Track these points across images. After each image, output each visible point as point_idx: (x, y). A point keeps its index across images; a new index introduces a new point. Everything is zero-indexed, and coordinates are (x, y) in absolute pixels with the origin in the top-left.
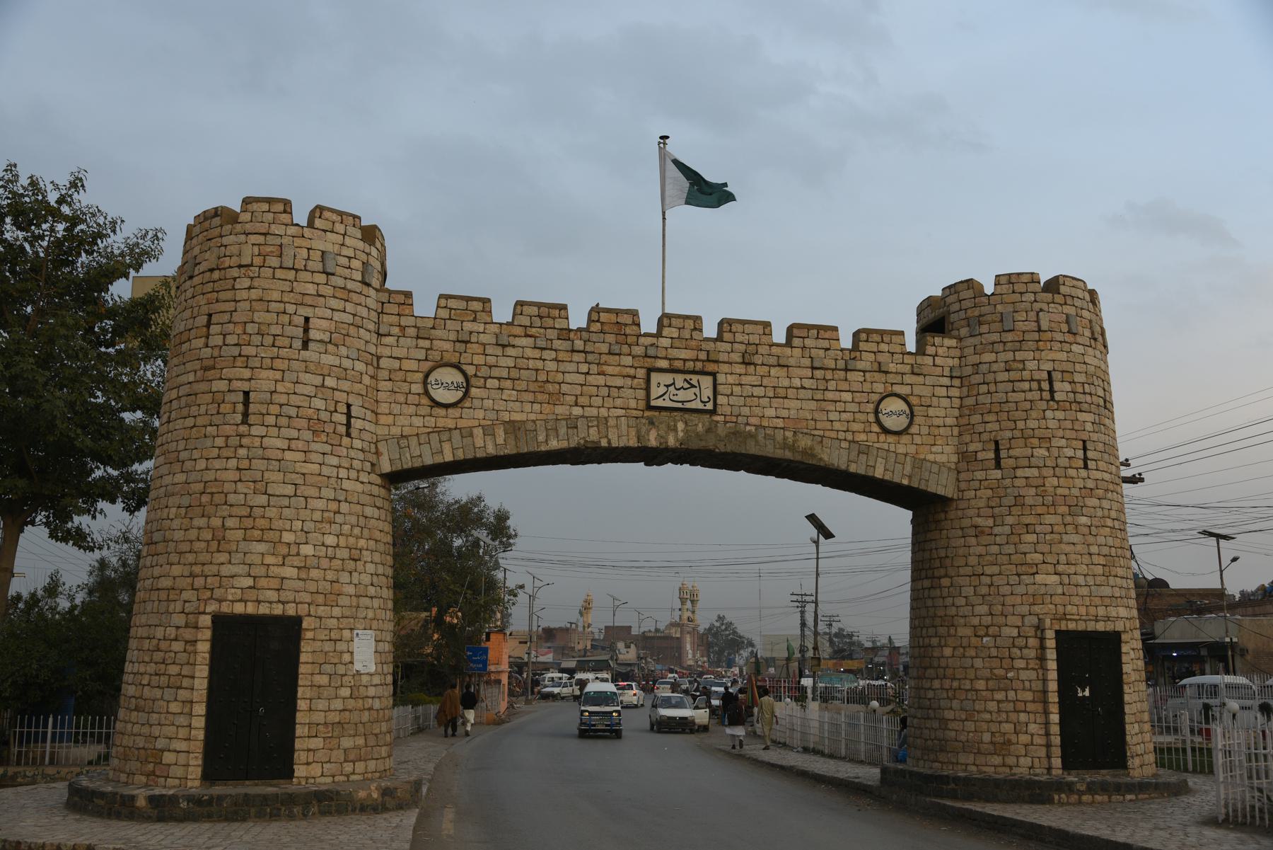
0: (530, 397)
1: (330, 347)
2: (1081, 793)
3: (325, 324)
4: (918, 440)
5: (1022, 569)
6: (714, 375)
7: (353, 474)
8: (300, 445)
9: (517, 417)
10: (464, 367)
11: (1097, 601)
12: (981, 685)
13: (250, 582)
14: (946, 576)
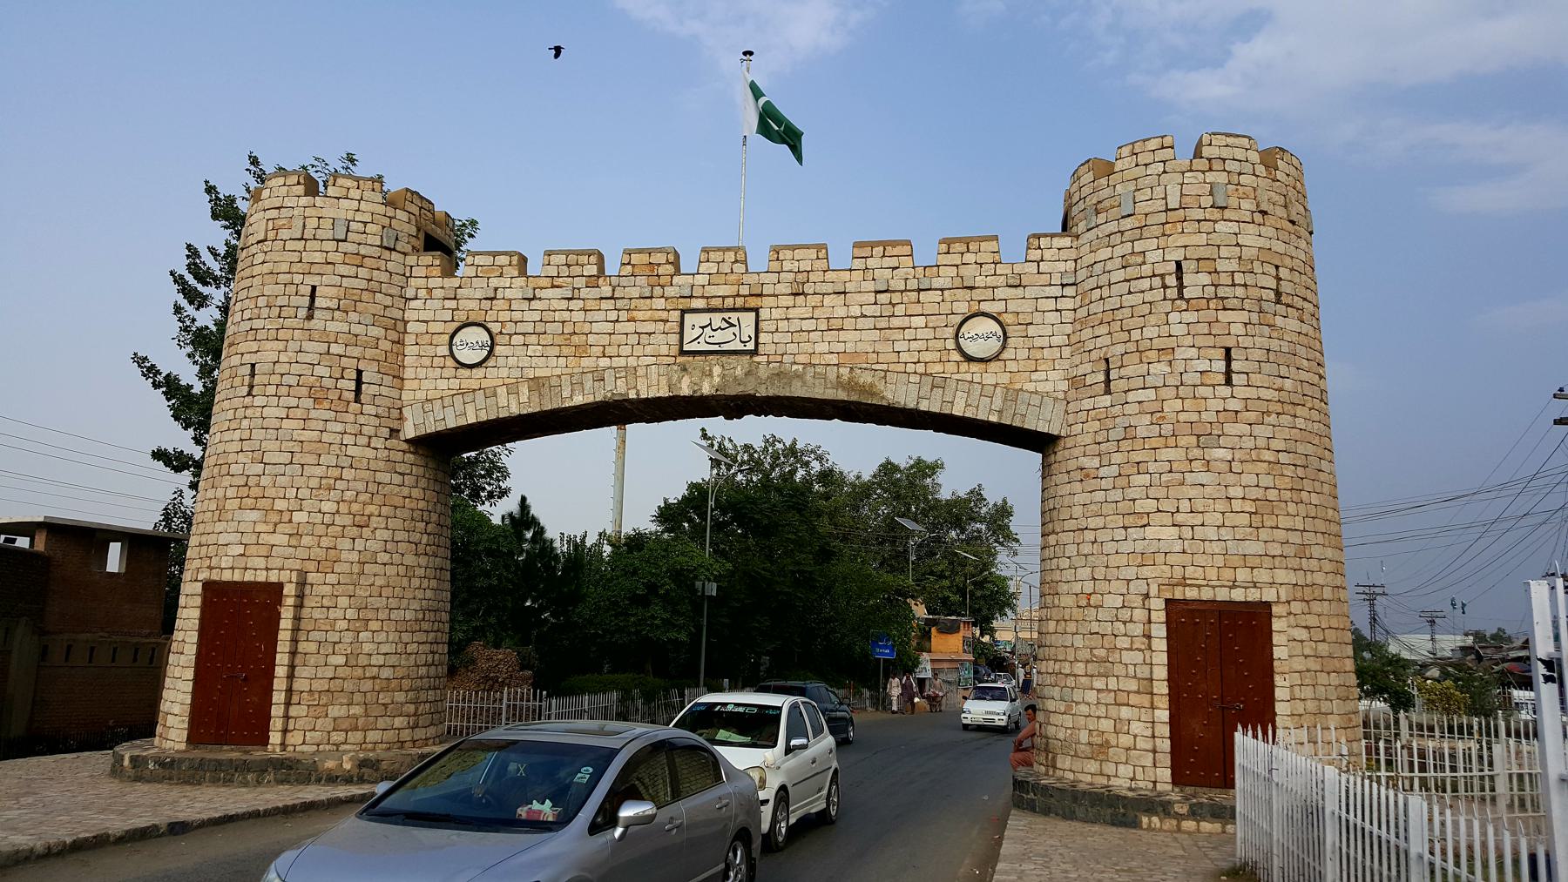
0: (556, 351)
1: (337, 313)
2: (1180, 817)
3: (333, 291)
4: (1012, 366)
5: (1129, 520)
6: (756, 310)
7: (363, 440)
8: (299, 413)
9: (539, 373)
10: (489, 325)
11: (1236, 561)
12: (1080, 668)
13: (241, 550)
14: (1053, 532)
